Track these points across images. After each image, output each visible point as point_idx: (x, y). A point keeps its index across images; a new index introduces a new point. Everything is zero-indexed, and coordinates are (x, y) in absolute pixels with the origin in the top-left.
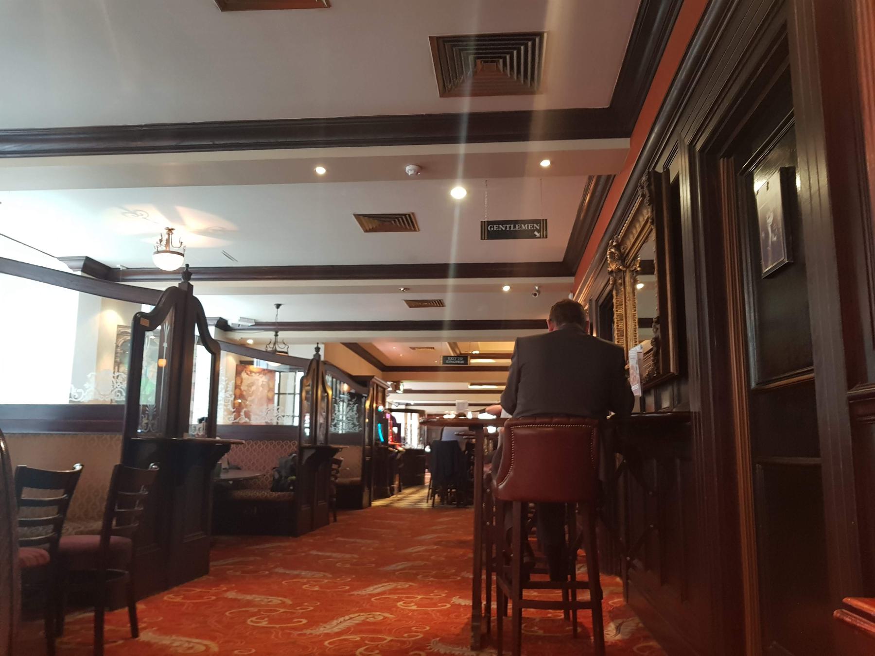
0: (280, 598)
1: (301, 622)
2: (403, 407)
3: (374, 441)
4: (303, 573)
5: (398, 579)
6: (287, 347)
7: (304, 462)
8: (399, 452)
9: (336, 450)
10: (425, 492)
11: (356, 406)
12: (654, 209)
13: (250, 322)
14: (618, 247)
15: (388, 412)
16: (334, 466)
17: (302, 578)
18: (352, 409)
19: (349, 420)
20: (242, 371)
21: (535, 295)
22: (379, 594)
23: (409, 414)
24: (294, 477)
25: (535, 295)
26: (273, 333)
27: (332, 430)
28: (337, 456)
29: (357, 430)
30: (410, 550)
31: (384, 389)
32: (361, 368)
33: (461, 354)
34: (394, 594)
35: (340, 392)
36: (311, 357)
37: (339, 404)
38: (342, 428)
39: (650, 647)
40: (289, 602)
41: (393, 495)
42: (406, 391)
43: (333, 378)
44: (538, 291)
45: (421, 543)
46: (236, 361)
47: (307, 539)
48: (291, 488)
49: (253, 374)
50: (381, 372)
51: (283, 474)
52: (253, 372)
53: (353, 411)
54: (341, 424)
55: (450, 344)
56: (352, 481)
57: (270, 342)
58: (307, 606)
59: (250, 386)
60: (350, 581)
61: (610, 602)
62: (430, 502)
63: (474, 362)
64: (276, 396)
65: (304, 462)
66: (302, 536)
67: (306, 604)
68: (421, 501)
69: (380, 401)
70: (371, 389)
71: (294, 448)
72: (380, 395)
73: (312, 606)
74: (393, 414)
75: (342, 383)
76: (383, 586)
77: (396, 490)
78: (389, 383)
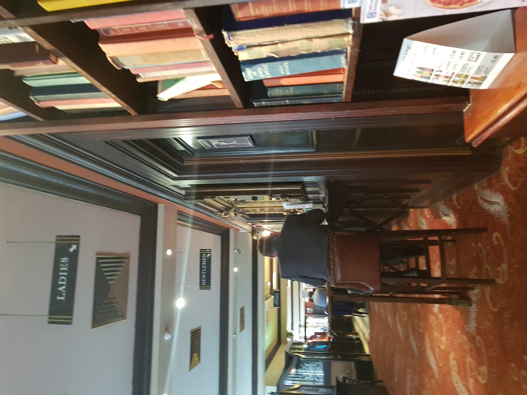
3: (328, 352)
5: (423, 345)
10: (357, 318)
12: (205, 197)
14: (221, 211)
16: (347, 382)
21: (240, 252)
22: (436, 359)
25: (240, 252)
27: (321, 382)
28: (341, 380)
29: (321, 363)
30: (401, 334)
32: (280, 359)
38: (320, 373)
39: (457, 198)
45: (395, 326)
61: (429, 217)
68: (364, 321)
72: (297, 346)
77: (357, 337)
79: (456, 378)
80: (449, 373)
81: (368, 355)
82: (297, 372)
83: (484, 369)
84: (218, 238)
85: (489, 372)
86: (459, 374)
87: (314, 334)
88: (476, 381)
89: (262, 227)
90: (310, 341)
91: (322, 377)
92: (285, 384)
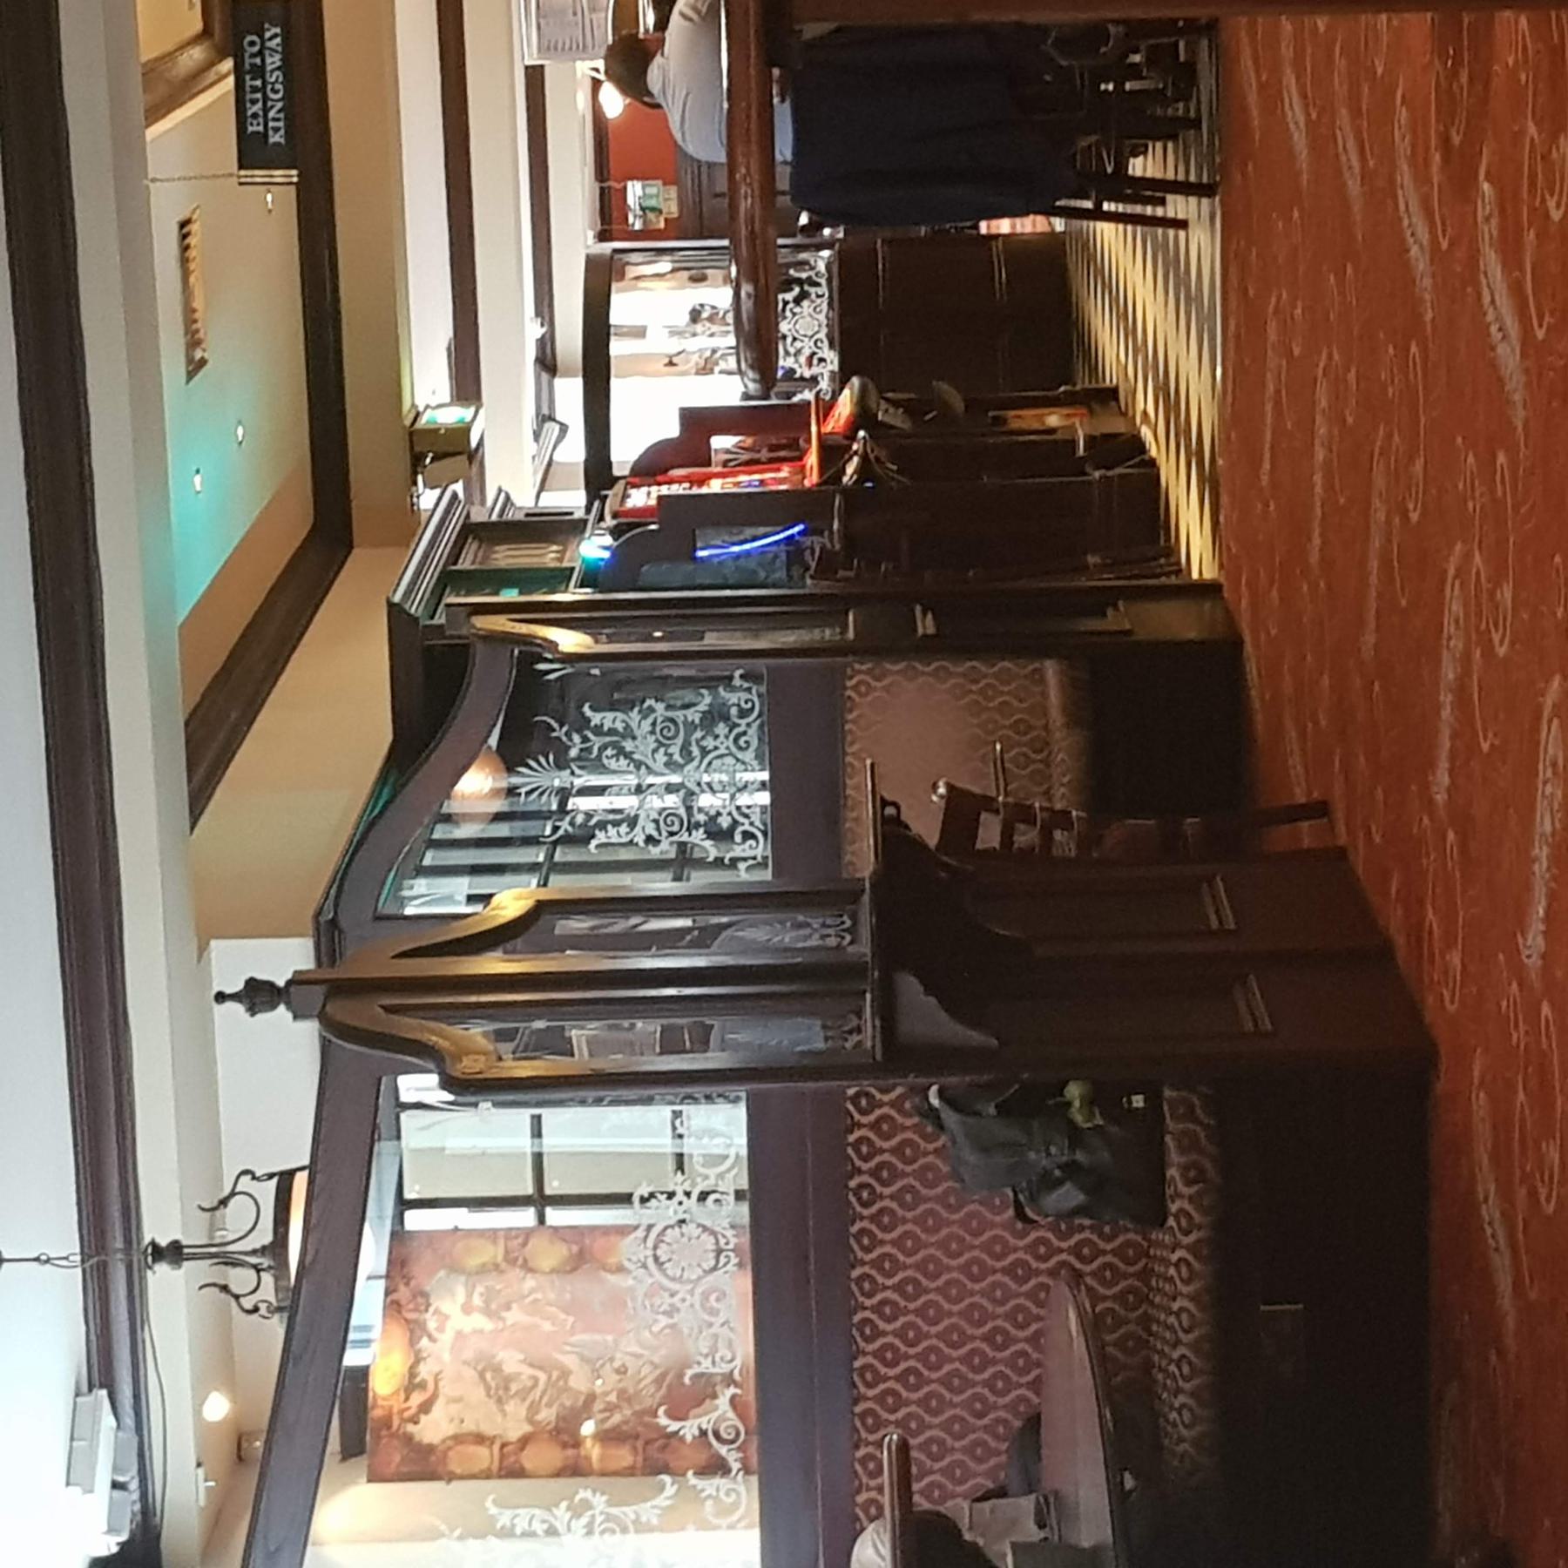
2: (570, 393)
3: (810, 585)
6: (245, 1183)
7: (976, 1037)
8: (863, 417)
9: (892, 831)
11: (596, 718)
13: (96, 1422)
15: (612, 494)
16: (989, 834)
18: (618, 742)
19: (685, 750)
20: (408, 1439)
23: (618, 347)
24: (1074, 1091)
26: (161, 1278)
28: (927, 827)
31: (470, 530)
35: (498, 817)
36: (310, 1029)
37: (589, 815)
41: (1138, 446)
42: (466, 384)
46: (345, 1485)
48: (1138, 1101)
49: (425, 1371)
50: (355, 551)
51: (1049, 1156)
52: (412, 1373)
53: (629, 733)
54: (705, 800)
55: (155, 112)
56: (1064, 710)
57: (225, 1288)
59: (499, 1387)
62: (1177, 206)
64: (555, 1216)
65: (976, 1037)
66: (1428, 1017)
68: (1172, 269)
69: (547, 556)
70: (484, 623)
71: (890, 1096)
72: (506, 557)
74: (625, 452)
75: (451, 807)
78: (427, 499)
81: (1208, 590)
82: (512, 792)
87: (672, 430)
90: (640, 498)
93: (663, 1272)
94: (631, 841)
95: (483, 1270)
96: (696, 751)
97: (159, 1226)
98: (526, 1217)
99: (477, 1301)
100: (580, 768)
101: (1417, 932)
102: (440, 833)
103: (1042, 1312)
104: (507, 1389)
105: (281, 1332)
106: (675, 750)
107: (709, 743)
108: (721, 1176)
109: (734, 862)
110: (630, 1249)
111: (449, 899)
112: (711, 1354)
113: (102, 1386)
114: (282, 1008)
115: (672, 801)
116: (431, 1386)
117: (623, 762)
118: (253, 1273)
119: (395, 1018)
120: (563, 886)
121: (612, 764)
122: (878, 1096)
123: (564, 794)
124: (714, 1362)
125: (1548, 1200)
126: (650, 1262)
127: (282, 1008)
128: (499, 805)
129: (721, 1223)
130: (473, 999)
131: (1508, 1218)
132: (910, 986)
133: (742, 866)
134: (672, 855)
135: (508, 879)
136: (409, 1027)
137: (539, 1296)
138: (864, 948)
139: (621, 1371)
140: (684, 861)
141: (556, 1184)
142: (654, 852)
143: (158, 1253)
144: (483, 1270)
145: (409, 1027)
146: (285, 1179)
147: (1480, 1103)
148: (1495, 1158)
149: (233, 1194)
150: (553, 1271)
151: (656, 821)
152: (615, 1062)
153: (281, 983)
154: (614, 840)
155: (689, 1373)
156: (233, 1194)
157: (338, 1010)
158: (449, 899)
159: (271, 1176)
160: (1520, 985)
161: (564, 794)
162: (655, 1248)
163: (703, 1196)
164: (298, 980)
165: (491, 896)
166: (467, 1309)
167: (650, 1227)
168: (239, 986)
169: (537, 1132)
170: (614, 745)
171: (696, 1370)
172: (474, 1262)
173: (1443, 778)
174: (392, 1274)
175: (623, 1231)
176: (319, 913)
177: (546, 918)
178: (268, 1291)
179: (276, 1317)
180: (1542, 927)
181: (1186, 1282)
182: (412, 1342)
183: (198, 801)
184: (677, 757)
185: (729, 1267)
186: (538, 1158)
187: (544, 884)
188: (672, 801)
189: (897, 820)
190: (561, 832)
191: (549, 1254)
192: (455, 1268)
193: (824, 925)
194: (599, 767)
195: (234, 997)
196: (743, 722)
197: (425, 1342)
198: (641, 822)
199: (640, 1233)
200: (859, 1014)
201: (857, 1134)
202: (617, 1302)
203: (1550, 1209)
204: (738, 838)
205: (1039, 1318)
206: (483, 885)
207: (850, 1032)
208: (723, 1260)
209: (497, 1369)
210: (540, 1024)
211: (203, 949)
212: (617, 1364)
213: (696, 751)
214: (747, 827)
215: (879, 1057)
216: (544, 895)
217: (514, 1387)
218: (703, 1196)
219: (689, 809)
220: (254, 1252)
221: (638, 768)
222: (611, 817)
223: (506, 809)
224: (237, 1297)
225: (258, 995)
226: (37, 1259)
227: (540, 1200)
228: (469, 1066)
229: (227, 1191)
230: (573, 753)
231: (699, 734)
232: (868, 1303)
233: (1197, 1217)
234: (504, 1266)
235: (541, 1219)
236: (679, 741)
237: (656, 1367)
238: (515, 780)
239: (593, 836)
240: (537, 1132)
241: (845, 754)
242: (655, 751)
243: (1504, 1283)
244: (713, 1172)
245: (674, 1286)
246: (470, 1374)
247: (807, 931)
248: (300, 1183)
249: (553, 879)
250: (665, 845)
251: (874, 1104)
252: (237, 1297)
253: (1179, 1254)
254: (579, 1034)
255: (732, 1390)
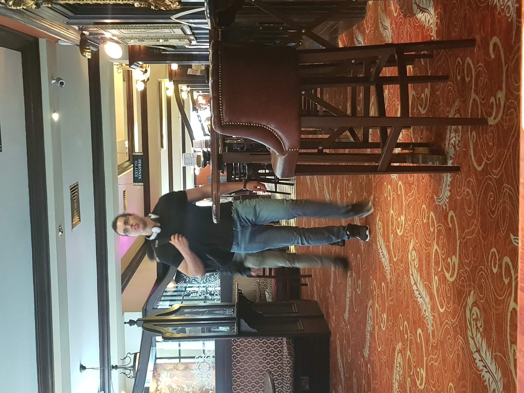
0: (396, 354)
1: (420, 334)
4: (369, 328)
6: (129, 355)
7: (254, 330)
9: (240, 294)
17: (374, 330)
21: (62, 84)
25: (62, 84)
26: (114, 372)
27: (217, 300)
33: (129, 160)
34: (388, 237)
35: (175, 291)
40: (399, 346)
43: (161, 301)
44: (58, 79)
47: (332, 325)
54: (210, 289)
57: (125, 373)
58: (403, 328)
60: (376, 282)
63: (138, 149)
65: (254, 330)
67: (401, 328)
73: (404, 322)
76: (381, 248)
79: (415, 276)
80: (407, 270)
82: (177, 287)
83: (455, 260)
84: (16, 56)
85: (461, 264)
86: (420, 270)
88: (443, 279)
89: (103, 34)
91: (218, 293)
92: (159, 307)
93: (200, 371)
94: (197, 296)
95: (170, 370)
96: (208, 281)
97: (114, 362)
98: (177, 361)
99: (169, 375)
100: (188, 283)
101: (328, 313)
102: (164, 294)
103: (265, 378)
104: (173, 391)
105: (134, 381)
106: (205, 280)
107: (210, 279)
108: (210, 354)
109: (214, 299)
110: (194, 366)
111: (165, 305)
112: (209, 384)
113: (103, 391)
114: (136, 325)
115: (204, 289)
116: (160, 390)
117: (196, 282)
118: (129, 371)
119: (155, 327)
120: (185, 303)
121: (194, 283)
122: (237, 340)
123: (186, 288)
124: (208, 387)
125: (349, 359)
126: (198, 369)
127: (136, 325)
128: (175, 289)
129: (210, 363)
130: (168, 323)
131: (343, 362)
132: (243, 321)
133: (215, 300)
134: (204, 298)
135: (176, 302)
136: (158, 328)
137: (179, 374)
138: (235, 315)
139: (193, 388)
140: (206, 299)
141: (183, 355)
142: (201, 298)
143: (113, 367)
144: (170, 370)
145: (158, 328)
146: (136, 354)
147: (338, 342)
148: (340, 352)
149: (126, 357)
150: (182, 370)
151: (201, 292)
152: (192, 334)
153: (136, 320)
154: (194, 295)
155: (204, 388)
156: (126, 357)
157: (145, 325)
158: (165, 305)
159: (133, 354)
160: (344, 322)
161: (186, 288)
162: (199, 366)
163: (207, 357)
164: (139, 320)
165: (172, 305)
166: (167, 377)
167: (198, 362)
168: (128, 321)
169: (179, 346)
170: (194, 279)
171: (206, 388)
172: (168, 368)
173: (332, 287)
174: (154, 370)
175: (194, 363)
176: (143, 308)
177: (181, 309)
178: (132, 374)
179: (133, 378)
180: (348, 313)
181: (289, 373)
182: (157, 382)
183: (123, 289)
184: (205, 281)
185: (211, 370)
186: (180, 350)
187: (182, 303)
188: (204, 289)
189: (241, 293)
190: (185, 294)
191: (181, 367)
192: (165, 370)
193: (229, 311)
194: (192, 283)
195: (128, 323)
196: (216, 276)
197: (159, 383)
198: (198, 293)
199: (196, 364)
200: (234, 326)
201: (234, 347)
202: (193, 375)
203: (349, 361)
204: (215, 295)
205: (264, 379)
206: (172, 303)
207: (233, 329)
208: (210, 369)
209: (172, 387)
210: (180, 328)
211: (123, 314)
212: (192, 386)
213: (208, 281)
214: (216, 294)
215: (237, 334)
216: (182, 305)
217: (175, 390)
218: (207, 357)
219: (207, 290)
220: (130, 367)
221: (198, 283)
222: (193, 291)
223: (176, 290)
224: (127, 375)
225: (131, 322)
226: (92, 368)
227: (180, 358)
228: (168, 335)
229: (126, 356)
230: (187, 281)
231: (209, 278)
232: (235, 376)
233: (291, 362)
234: (173, 369)
235: (180, 361)
236: (205, 279)
237: (199, 387)
238: (178, 285)
239: (190, 295)
240: (179, 346)
241: (233, 281)
242: (201, 280)
243: (342, 374)
244: (209, 353)
245: (202, 373)
246: (167, 388)
247: (226, 312)
248: (138, 355)
249: (184, 302)
250: (202, 296)
251: (236, 342)
252: (127, 375)
253: (288, 368)
254: (187, 329)
255: (212, 392)
